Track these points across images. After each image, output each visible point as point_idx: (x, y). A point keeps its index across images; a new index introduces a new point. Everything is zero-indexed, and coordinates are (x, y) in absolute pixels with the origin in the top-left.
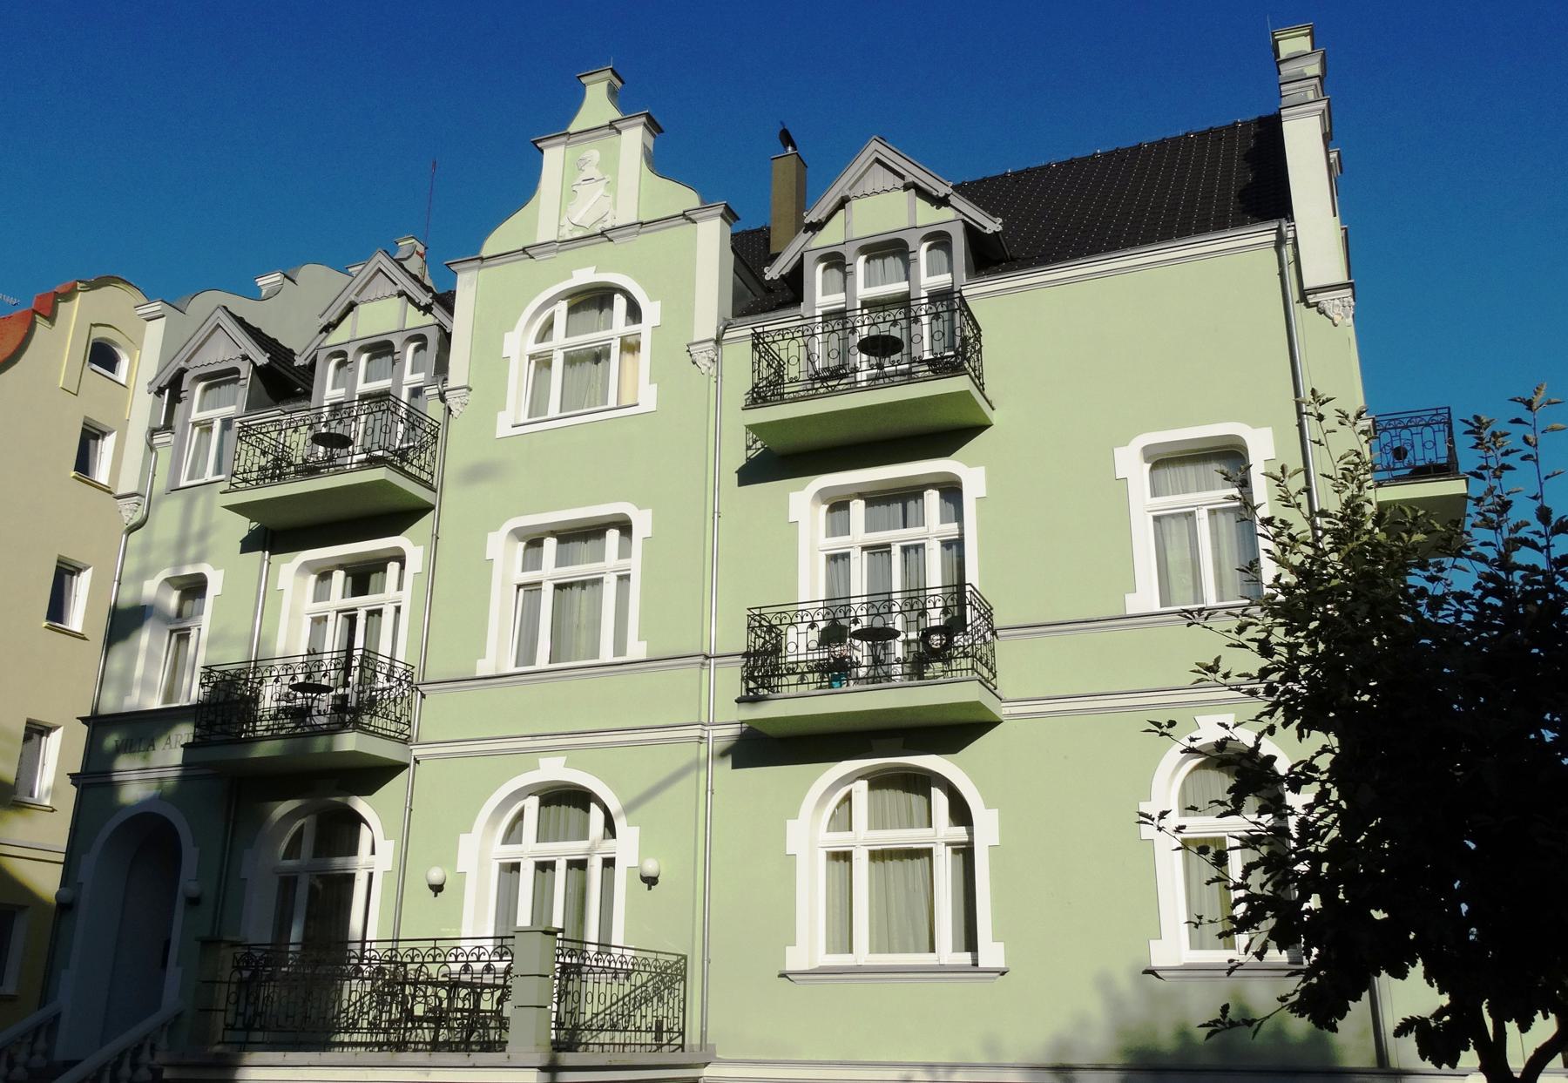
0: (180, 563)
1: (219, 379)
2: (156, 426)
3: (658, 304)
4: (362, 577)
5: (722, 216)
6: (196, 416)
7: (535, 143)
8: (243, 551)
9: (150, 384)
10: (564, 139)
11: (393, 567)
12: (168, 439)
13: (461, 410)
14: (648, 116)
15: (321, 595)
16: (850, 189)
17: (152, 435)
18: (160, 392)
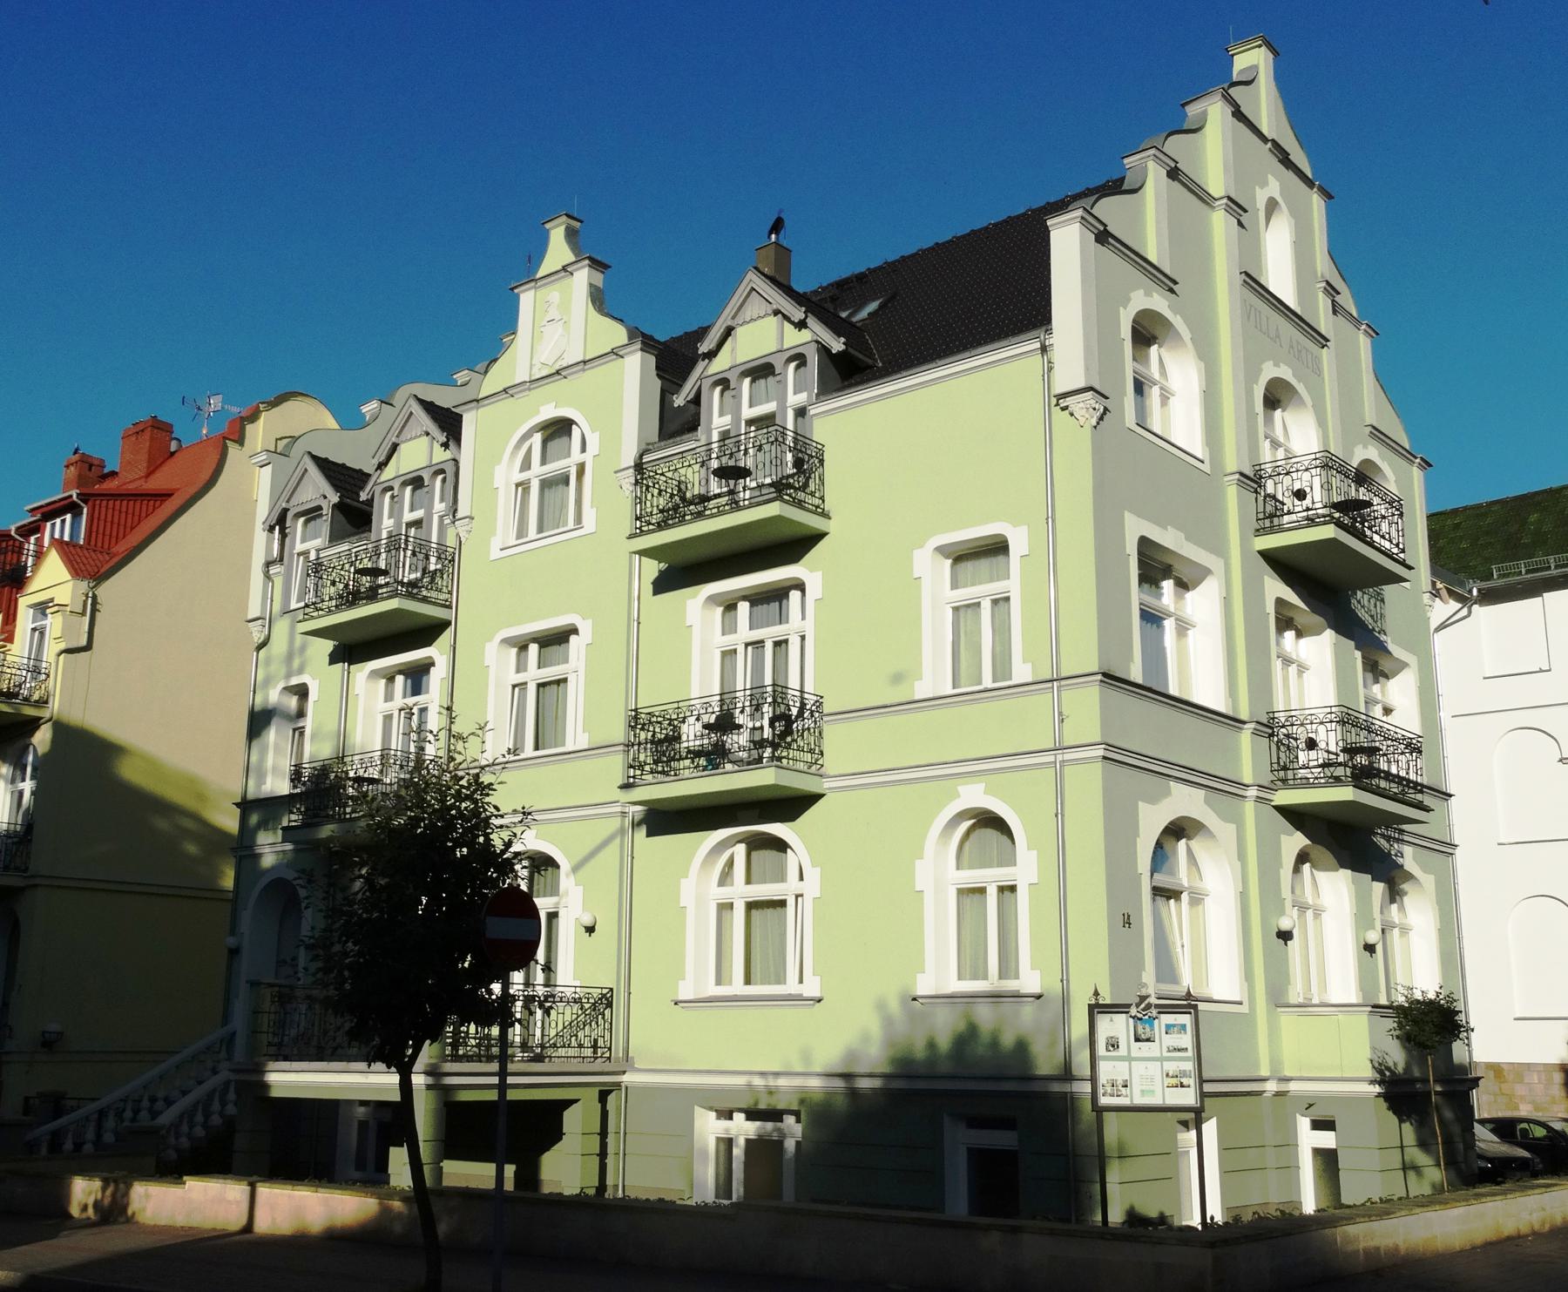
0: (288, 676)
1: (312, 514)
2: (271, 559)
3: (597, 434)
4: (417, 676)
5: (641, 349)
6: (299, 547)
7: (512, 289)
8: (331, 663)
9: (264, 523)
10: (533, 284)
11: (795, 595)
12: (278, 570)
13: (467, 536)
14: (590, 258)
15: (729, 628)
16: (733, 318)
17: (268, 567)
18: (271, 529)
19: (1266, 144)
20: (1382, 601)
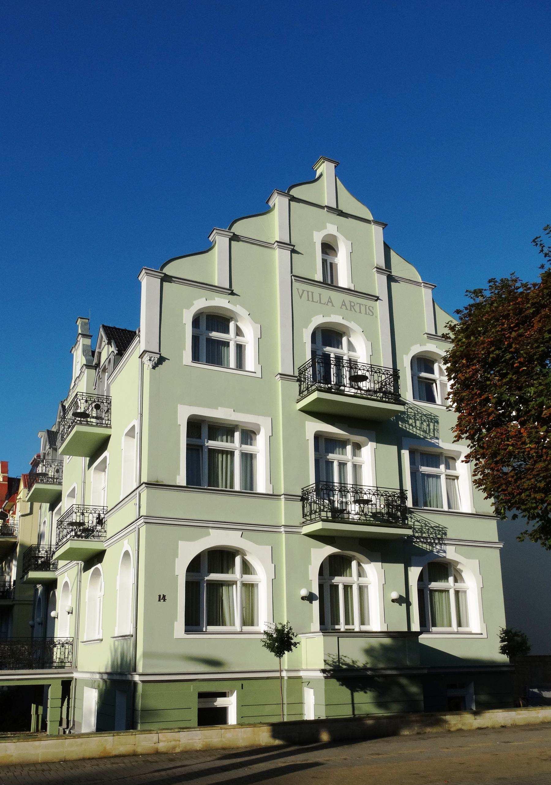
19: (324, 209)
20: (437, 422)
